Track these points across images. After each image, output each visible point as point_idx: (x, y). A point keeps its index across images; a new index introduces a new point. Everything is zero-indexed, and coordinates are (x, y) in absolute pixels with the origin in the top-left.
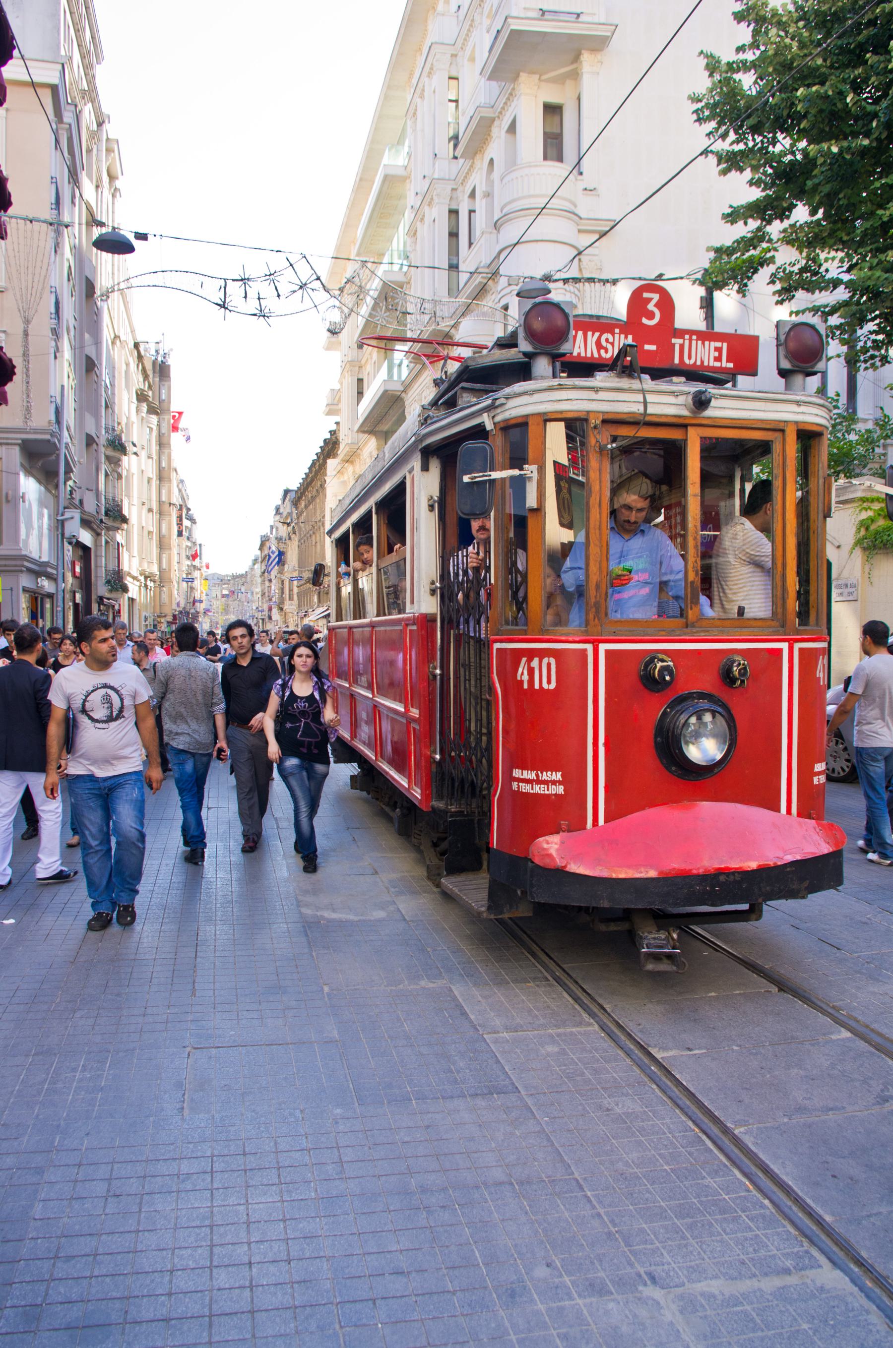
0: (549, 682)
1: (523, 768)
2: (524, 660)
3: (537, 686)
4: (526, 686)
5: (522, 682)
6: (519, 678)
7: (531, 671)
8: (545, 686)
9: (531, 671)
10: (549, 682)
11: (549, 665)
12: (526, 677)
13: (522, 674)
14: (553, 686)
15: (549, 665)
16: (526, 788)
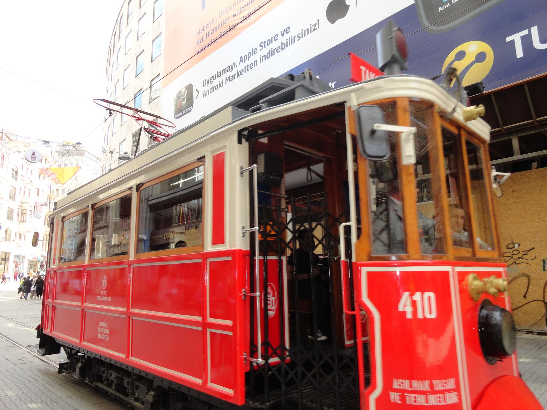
0: (430, 313)
1: (411, 378)
2: (406, 295)
3: (420, 316)
4: (409, 316)
5: (404, 313)
6: (401, 308)
7: (414, 304)
8: (428, 316)
9: (414, 304)
10: (430, 313)
11: (429, 298)
12: (409, 310)
13: (405, 306)
14: (433, 316)
15: (429, 298)
16: (421, 400)
